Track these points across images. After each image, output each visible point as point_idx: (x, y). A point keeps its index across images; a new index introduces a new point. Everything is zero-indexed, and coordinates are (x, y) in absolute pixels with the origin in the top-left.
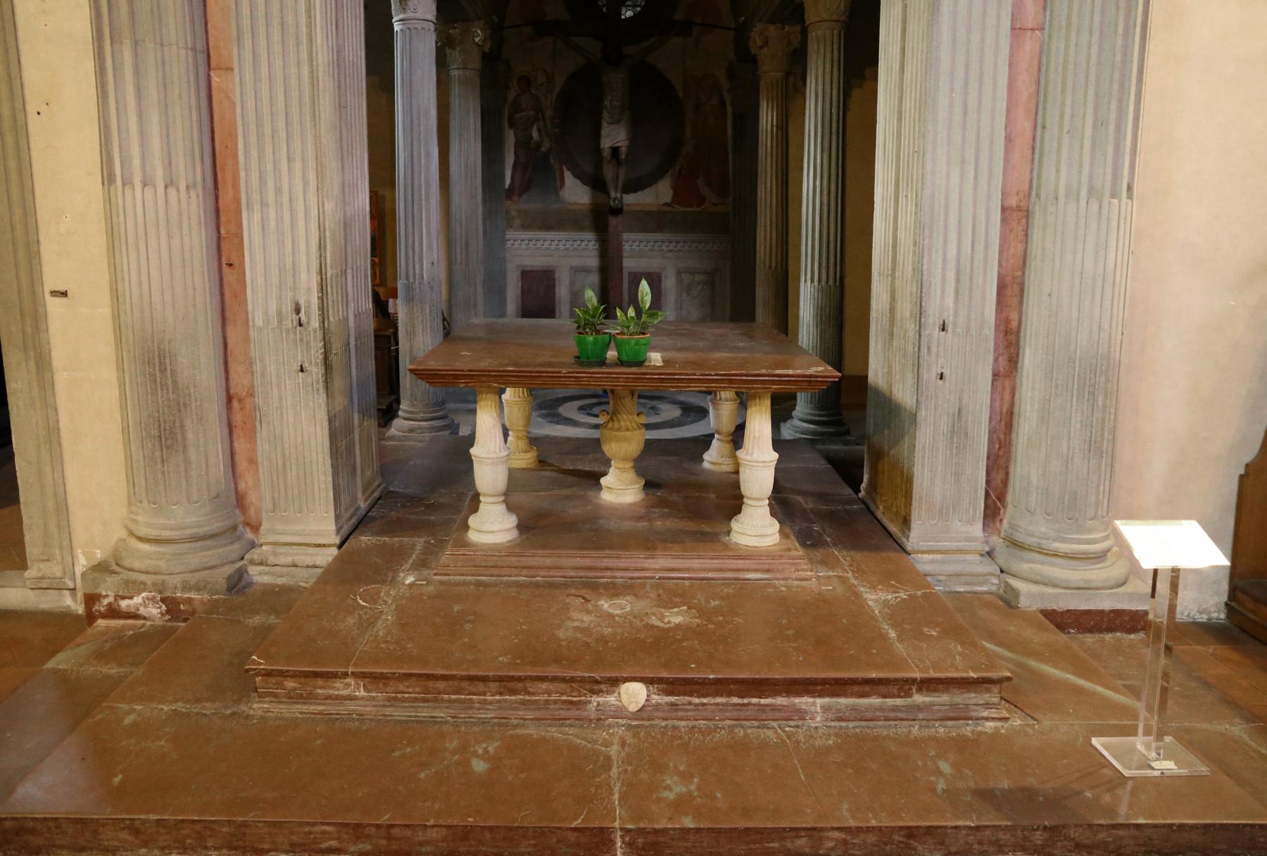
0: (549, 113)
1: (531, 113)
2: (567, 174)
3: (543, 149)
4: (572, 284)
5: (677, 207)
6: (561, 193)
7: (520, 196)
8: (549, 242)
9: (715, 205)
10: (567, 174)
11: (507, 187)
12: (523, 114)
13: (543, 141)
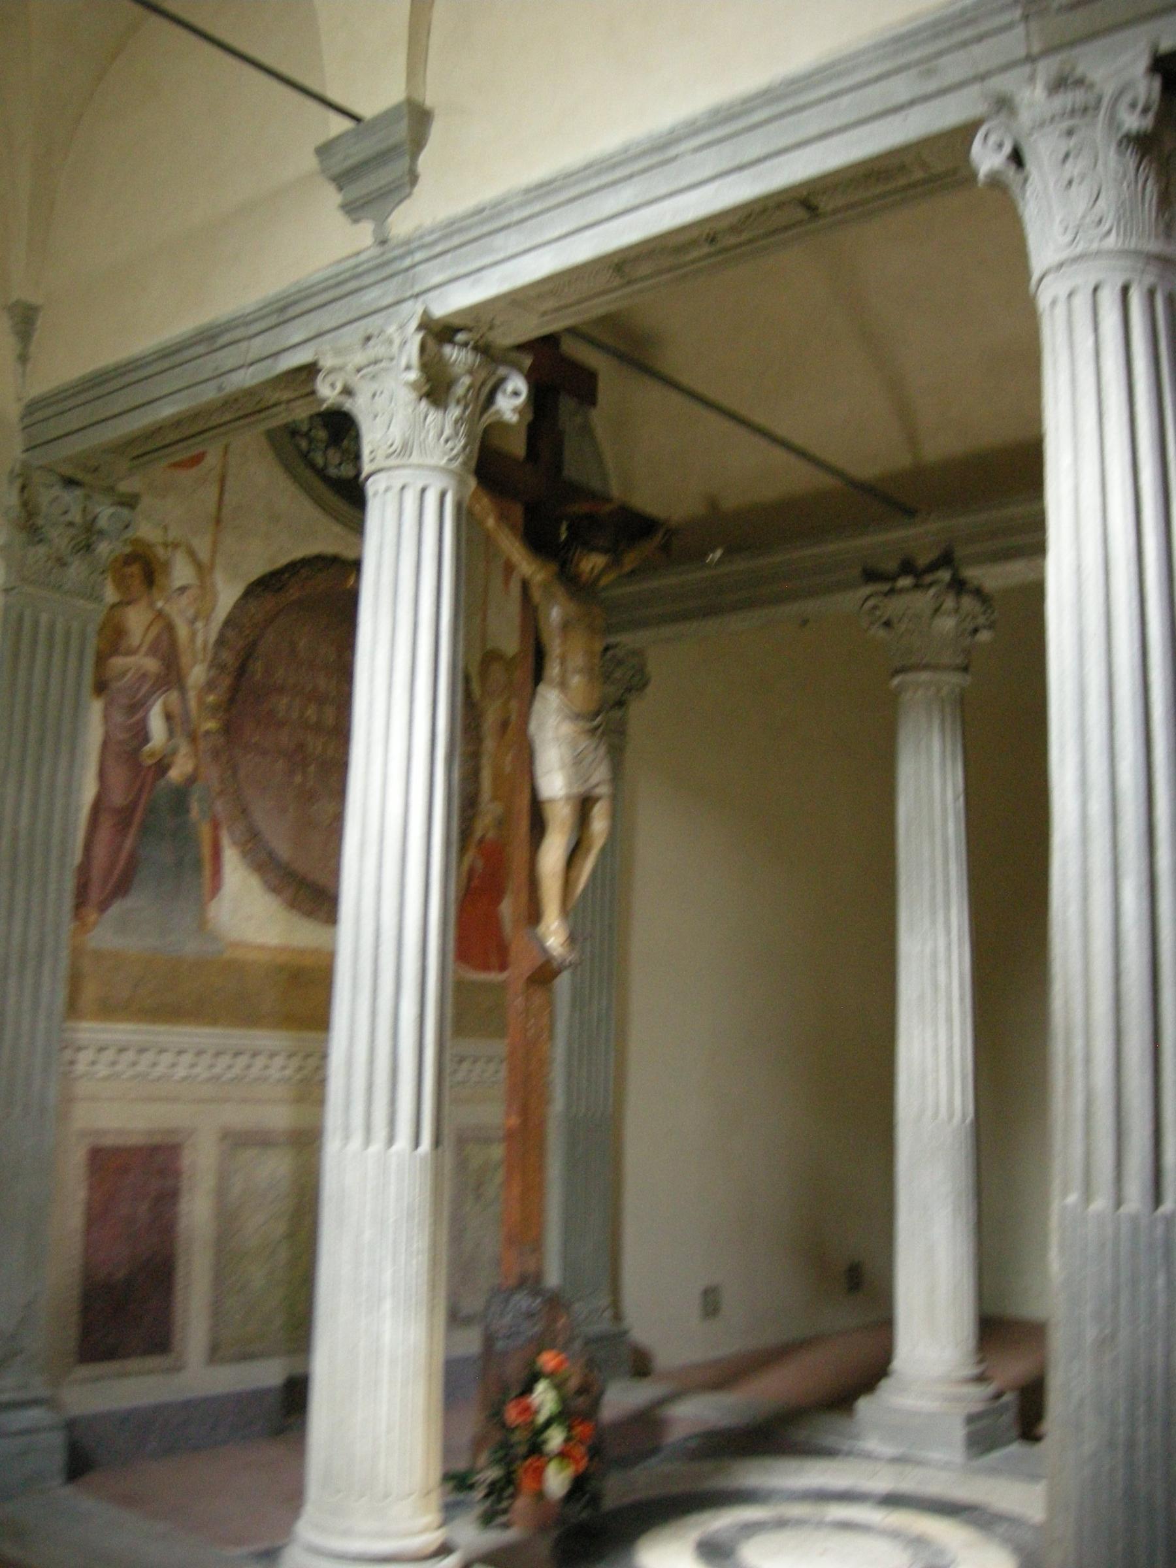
0: (197, 674)
1: (151, 665)
2: (231, 858)
3: (175, 774)
4: (221, 1192)
7: (103, 907)
10: (231, 858)
12: (130, 660)
13: (174, 752)
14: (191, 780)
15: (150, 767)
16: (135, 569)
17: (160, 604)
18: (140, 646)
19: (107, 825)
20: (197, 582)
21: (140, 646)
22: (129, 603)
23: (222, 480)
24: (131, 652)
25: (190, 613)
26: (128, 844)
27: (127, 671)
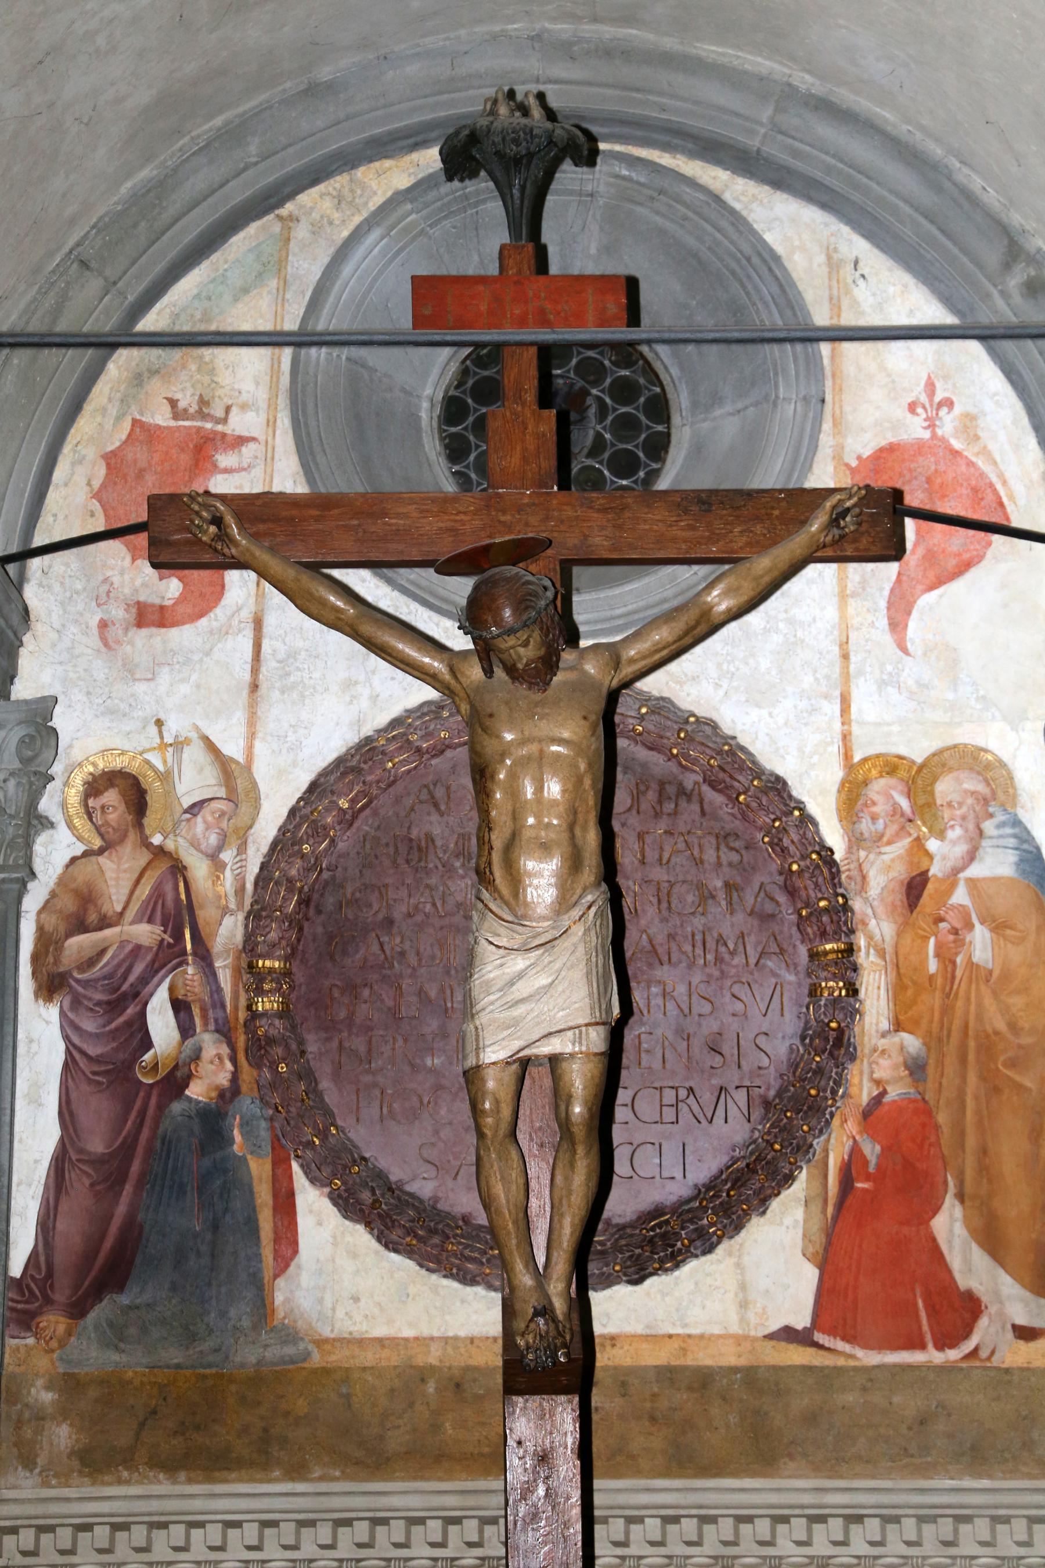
1: (146, 933)
3: (196, 1091)
5: (841, 1345)
6: (280, 1294)
7: (78, 1310)
8: (214, 1535)
9: (1025, 1333)
11: (16, 1270)
12: (107, 932)
13: (197, 1056)
14: (229, 1094)
15: (151, 1086)
16: (111, 797)
17: (157, 840)
18: (121, 914)
19: (80, 1183)
20: (222, 793)
21: (121, 914)
22: (101, 851)
23: (258, 623)
24: (104, 923)
25: (213, 839)
26: (121, 1209)
27: (103, 952)
